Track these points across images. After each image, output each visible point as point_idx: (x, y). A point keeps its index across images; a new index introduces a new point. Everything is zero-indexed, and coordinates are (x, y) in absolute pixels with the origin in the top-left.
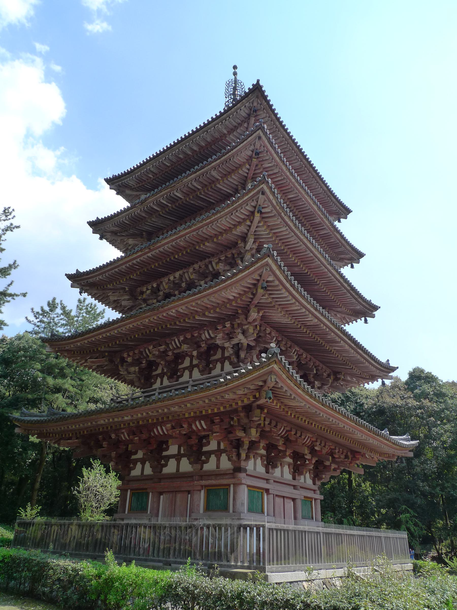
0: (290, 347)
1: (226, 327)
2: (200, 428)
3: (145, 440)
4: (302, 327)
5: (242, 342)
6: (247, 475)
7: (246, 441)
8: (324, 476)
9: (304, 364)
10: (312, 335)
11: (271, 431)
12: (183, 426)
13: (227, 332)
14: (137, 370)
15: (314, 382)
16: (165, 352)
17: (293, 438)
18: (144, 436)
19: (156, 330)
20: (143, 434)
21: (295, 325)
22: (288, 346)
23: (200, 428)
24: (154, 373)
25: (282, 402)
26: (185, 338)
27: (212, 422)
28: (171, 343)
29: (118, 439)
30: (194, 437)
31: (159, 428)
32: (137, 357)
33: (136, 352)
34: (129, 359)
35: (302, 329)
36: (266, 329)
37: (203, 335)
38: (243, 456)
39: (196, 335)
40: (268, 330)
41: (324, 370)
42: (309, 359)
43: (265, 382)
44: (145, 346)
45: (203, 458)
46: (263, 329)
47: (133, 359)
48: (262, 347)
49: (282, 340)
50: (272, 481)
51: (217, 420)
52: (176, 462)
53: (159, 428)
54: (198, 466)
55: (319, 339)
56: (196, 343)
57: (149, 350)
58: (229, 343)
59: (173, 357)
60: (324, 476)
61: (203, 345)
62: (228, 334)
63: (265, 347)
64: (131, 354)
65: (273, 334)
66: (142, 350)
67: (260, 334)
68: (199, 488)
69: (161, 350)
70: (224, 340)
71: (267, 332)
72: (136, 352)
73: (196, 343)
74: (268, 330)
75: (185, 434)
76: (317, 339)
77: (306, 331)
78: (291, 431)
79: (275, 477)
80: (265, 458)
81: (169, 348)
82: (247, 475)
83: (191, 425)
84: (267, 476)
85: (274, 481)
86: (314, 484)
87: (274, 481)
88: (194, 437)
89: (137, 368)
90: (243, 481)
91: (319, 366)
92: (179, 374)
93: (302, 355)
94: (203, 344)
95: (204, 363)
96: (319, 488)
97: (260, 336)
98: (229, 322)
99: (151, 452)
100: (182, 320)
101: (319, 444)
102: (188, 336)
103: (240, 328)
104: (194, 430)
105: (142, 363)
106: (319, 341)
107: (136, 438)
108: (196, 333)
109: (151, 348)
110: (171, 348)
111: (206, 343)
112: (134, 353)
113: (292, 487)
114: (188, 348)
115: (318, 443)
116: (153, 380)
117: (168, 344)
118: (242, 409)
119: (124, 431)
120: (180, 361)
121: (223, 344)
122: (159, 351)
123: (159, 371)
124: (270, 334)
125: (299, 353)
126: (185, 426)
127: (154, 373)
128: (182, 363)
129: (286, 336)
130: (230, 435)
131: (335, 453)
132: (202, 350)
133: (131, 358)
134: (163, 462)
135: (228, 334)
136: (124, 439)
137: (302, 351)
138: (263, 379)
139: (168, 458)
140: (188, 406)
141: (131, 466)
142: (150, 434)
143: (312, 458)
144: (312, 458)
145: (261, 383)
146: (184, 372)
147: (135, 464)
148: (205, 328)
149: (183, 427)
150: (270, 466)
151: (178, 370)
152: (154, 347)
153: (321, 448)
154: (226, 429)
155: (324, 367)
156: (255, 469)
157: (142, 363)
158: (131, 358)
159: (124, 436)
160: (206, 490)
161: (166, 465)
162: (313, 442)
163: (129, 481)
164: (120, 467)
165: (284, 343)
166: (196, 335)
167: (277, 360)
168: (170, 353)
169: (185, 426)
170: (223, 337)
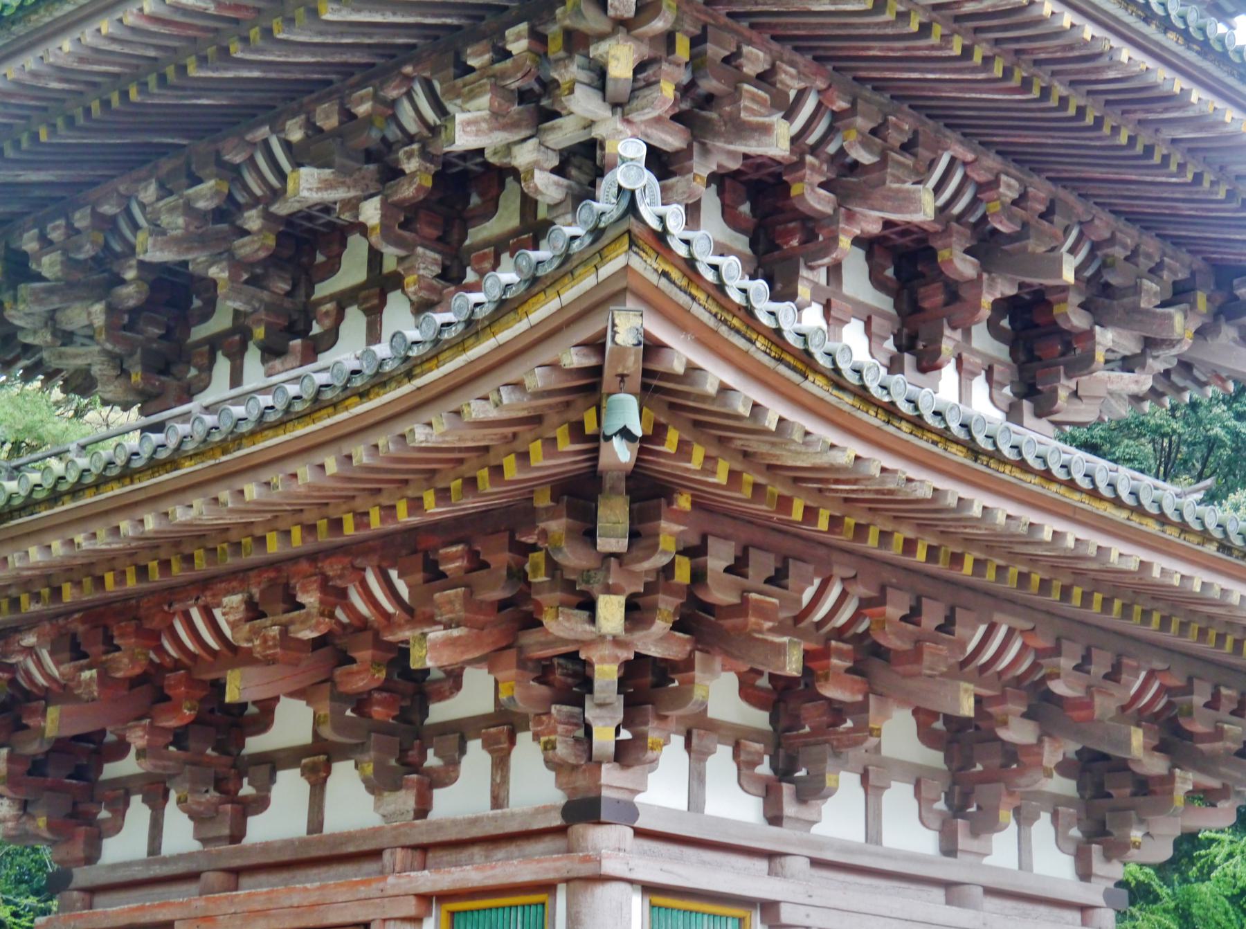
0: (907, 148)
1: (508, 54)
2: (389, 607)
3: (135, 682)
4: (938, 30)
5: (597, 132)
6: (640, 833)
7: (603, 660)
8: (1136, 835)
9: (1011, 238)
10: (1008, 73)
11: (741, 608)
12: (302, 598)
13: (514, 84)
14: (99, 320)
15: (1089, 335)
16: (227, 212)
17: (891, 641)
18: (125, 665)
19: (134, 95)
20: (118, 649)
21: (889, 16)
22: (896, 138)
23: (389, 607)
24: (200, 332)
25: (746, 454)
26: (313, 130)
27: (434, 575)
28: (251, 161)
29: (13, 682)
30: (364, 655)
31: (195, 614)
32: (87, 251)
33: (81, 219)
34: (46, 260)
35: (935, 39)
36: (737, 54)
37: (406, 105)
38: (604, 737)
39: (363, 109)
40: (755, 59)
41: (1144, 264)
42: (1042, 208)
43: (597, 345)
44: (122, 188)
45: (432, 760)
46: (715, 51)
47: (70, 263)
48: (732, 154)
49: (852, 111)
50: (798, 865)
51: (453, 560)
52: (304, 787)
53: (195, 614)
54: (406, 800)
55: (1060, 90)
56: (370, 156)
57: (143, 206)
58: (532, 143)
59: (271, 241)
60: (1136, 835)
61: (411, 166)
62: (523, 96)
63: (746, 156)
64: (56, 235)
65: (790, 81)
66: (108, 209)
67: (709, 84)
68: (410, 907)
69: (201, 205)
70: (504, 128)
71: (750, 69)
72: (81, 219)
73: (370, 156)
74: (755, 59)
75: (318, 643)
76: (1046, 92)
77: (967, 52)
78: (880, 600)
79: (821, 843)
80: (758, 747)
81: (246, 187)
82: (640, 833)
83: (343, 594)
84: (769, 838)
85: (816, 863)
86: (1085, 874)
87: (816, 863)
88: (364, 655)
89: (98, 308)
90: (610, 866)
91: (1112, 241)
92: (316, 329)
93: (994, 184)
94: (410, 156)
95: (427, 263)
96: (1107, 895)
97: (709, 100)
98: (523, 27)
99: (179, 738)
100: (254, 33)
101: (1077, 668)
102: (328, 118)
103: (578, 59)
104: (364, 620)
105: (123, 282)
106: (1064, 101)
107: (86, 675)
108: (362, 100)
109: (149, 193)
110: (258, 192)
111: (425, 155)
112: (72, 231)
113: (939, 894)
114: (328, 185)
115: (1066, 663)
116: (193, 372)
117: (236, 168)
118: (555, 498)
119: (30, 640)
120: (320, 258)
121: (508, 147)
122: (188, 209)
123: (220, 322)
124: (765, 79)
125: (981, 176)
126: (310, 599)
127: (200, 332)
128: (332, 268)
129: (879, 86)
130: (530, 638)
131: (1189, 713)
132: (407, 191)
133: (56, 256)
134: (247, 790)
135: (523, 96)
136: (40, 680)
137: (992, 162)
138: (586, 331)
139: (272, 762)
140: (248, 497)
141: (104, 814)
142: (160, 650)
143: (1040, 741)
144: (1040, 741)
145: (575, 359)
146: (340, 317)
147: (120, 807)
148: (408, 69)
149: (301, 606)
150: (787, 789)
151: (309, 312)
152: (165, 190)
153: (1089, 688)
154: (503, 605)
155: (1151, 245)
156: (695, 801)
157: (123, 282)
158: (56, 256)
159: (39, 663)
160: (444, 917)
161: (260, 803)
162: (1041, 653)
163: (93, 891)
164: (42, 822)
165: (862, 123)
166: (363, 109)
167: (637, 228)
168: (252, 220)
169: (310, 599)
170: (495, 114)
